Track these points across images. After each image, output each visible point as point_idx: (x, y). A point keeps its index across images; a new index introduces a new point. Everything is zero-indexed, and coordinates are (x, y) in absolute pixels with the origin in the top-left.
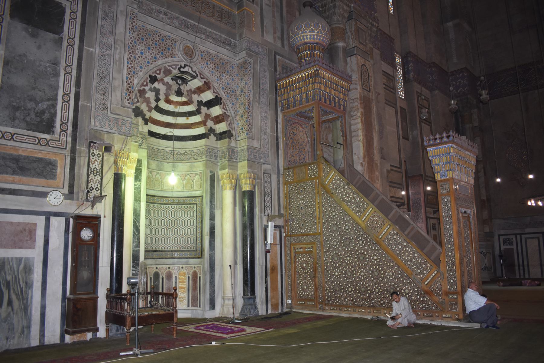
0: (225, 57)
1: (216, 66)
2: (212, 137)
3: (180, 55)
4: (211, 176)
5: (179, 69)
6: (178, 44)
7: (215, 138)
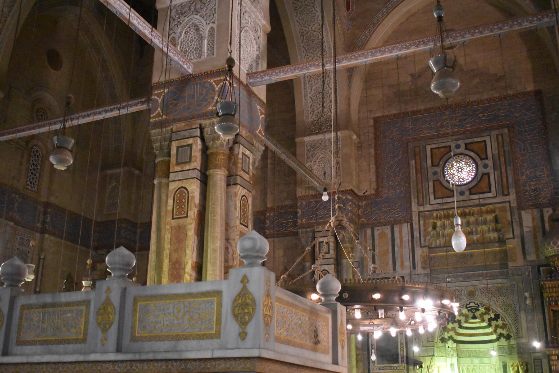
0: (500, 285)
1: (493, 294)
2: (503, 340)
3: (465, 298)
4: (503, 366)
5: (466, 307)
6: (463, 292)
7: (505, 339)
